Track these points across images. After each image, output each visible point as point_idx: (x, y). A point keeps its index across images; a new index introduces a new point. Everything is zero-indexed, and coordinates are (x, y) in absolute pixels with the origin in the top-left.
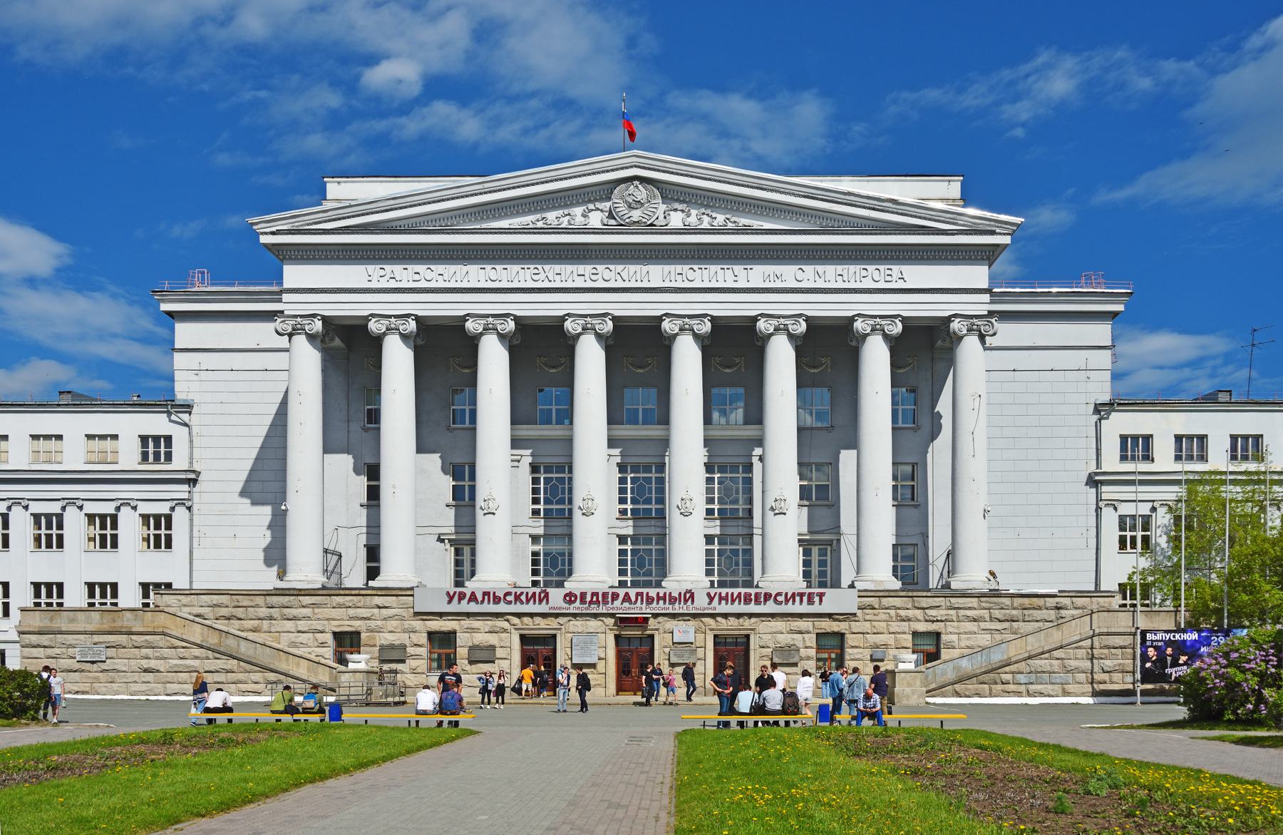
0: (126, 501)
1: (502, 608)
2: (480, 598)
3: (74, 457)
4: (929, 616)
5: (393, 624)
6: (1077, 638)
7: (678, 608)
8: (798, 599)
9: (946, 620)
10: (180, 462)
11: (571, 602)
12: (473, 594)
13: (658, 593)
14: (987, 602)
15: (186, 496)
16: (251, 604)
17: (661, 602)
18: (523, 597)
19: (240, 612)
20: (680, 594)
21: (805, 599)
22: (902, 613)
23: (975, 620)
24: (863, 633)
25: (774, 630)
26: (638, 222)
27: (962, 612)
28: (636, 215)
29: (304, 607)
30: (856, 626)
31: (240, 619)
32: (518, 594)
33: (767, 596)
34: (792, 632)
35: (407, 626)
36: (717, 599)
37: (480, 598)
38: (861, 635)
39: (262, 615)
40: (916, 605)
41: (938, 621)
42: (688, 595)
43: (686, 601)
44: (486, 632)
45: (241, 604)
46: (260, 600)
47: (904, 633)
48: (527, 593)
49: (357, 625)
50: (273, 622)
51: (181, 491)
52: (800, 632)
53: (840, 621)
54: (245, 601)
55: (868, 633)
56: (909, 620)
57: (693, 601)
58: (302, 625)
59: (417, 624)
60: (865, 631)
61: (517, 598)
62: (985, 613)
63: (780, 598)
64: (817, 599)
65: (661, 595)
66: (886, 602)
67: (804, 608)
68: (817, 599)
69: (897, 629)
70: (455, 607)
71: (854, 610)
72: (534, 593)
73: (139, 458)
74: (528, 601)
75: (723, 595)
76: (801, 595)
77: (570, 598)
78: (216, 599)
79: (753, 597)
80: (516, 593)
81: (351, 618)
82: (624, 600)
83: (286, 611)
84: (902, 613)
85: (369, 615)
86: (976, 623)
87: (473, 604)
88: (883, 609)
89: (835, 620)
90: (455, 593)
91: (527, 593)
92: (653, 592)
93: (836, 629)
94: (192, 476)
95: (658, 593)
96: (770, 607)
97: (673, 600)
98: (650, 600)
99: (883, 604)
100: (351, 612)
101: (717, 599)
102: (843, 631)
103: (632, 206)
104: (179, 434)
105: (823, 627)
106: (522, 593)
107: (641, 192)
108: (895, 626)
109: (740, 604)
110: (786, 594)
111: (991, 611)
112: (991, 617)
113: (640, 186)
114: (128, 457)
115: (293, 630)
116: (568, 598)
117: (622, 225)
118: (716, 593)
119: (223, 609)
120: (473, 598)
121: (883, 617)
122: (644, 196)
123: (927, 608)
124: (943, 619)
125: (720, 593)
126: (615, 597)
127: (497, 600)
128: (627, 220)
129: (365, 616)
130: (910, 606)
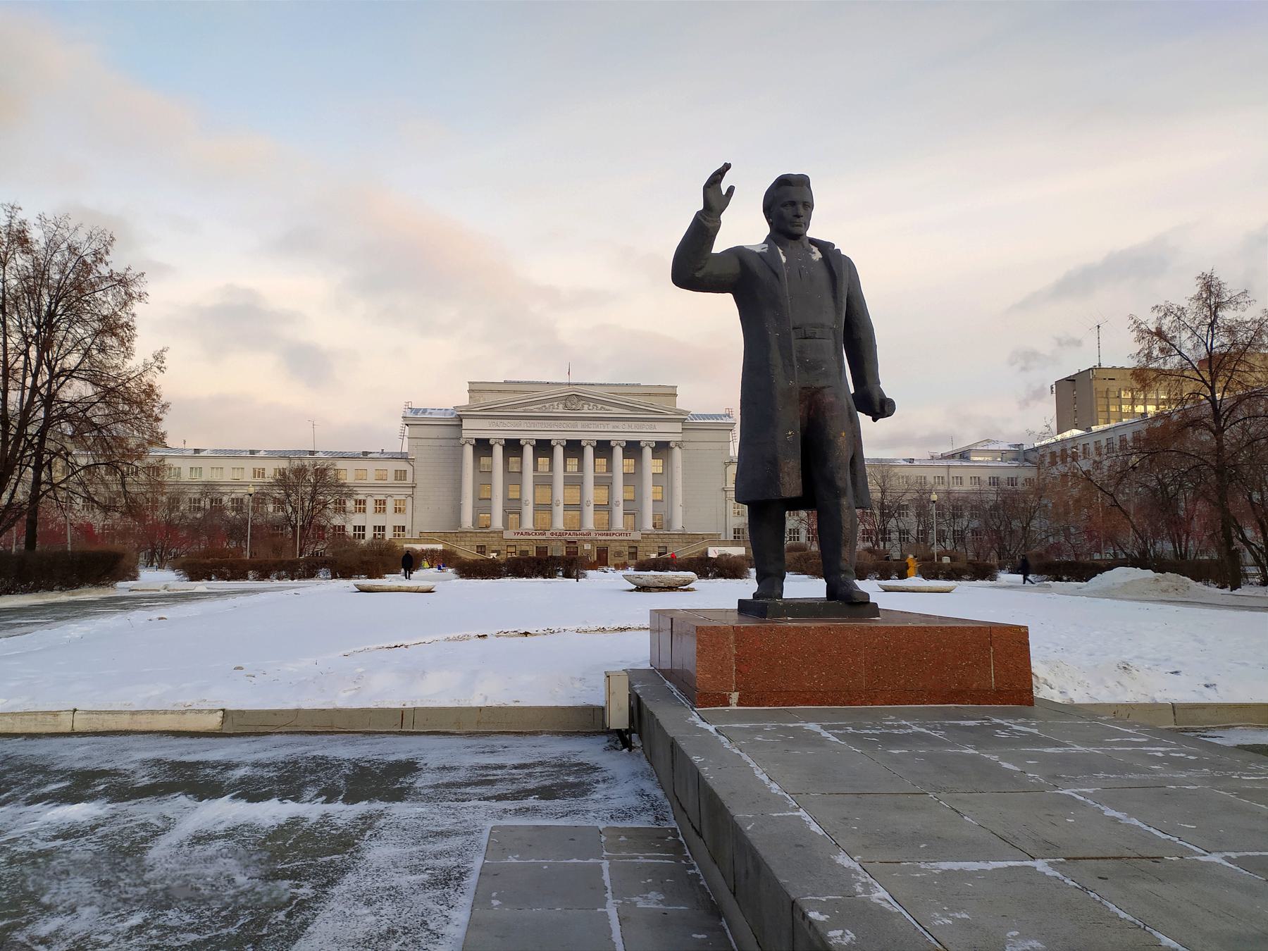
1: (531, 537)
3: (371, 479)
10: (409, 480)
33: (613, 534)
49: (485, 543)
51: (409, 491)
59: (504, 543)
61: (536, 534)
67: (625, 538)
77: (552, 534)
92: (578, 533)
96: (614, 537)
97: (584, 535)
98: (577, 535)
104: (409, 470)
114: (391, 479)
120: (522, 534)
126: (566, 534)
127: (529, 535)
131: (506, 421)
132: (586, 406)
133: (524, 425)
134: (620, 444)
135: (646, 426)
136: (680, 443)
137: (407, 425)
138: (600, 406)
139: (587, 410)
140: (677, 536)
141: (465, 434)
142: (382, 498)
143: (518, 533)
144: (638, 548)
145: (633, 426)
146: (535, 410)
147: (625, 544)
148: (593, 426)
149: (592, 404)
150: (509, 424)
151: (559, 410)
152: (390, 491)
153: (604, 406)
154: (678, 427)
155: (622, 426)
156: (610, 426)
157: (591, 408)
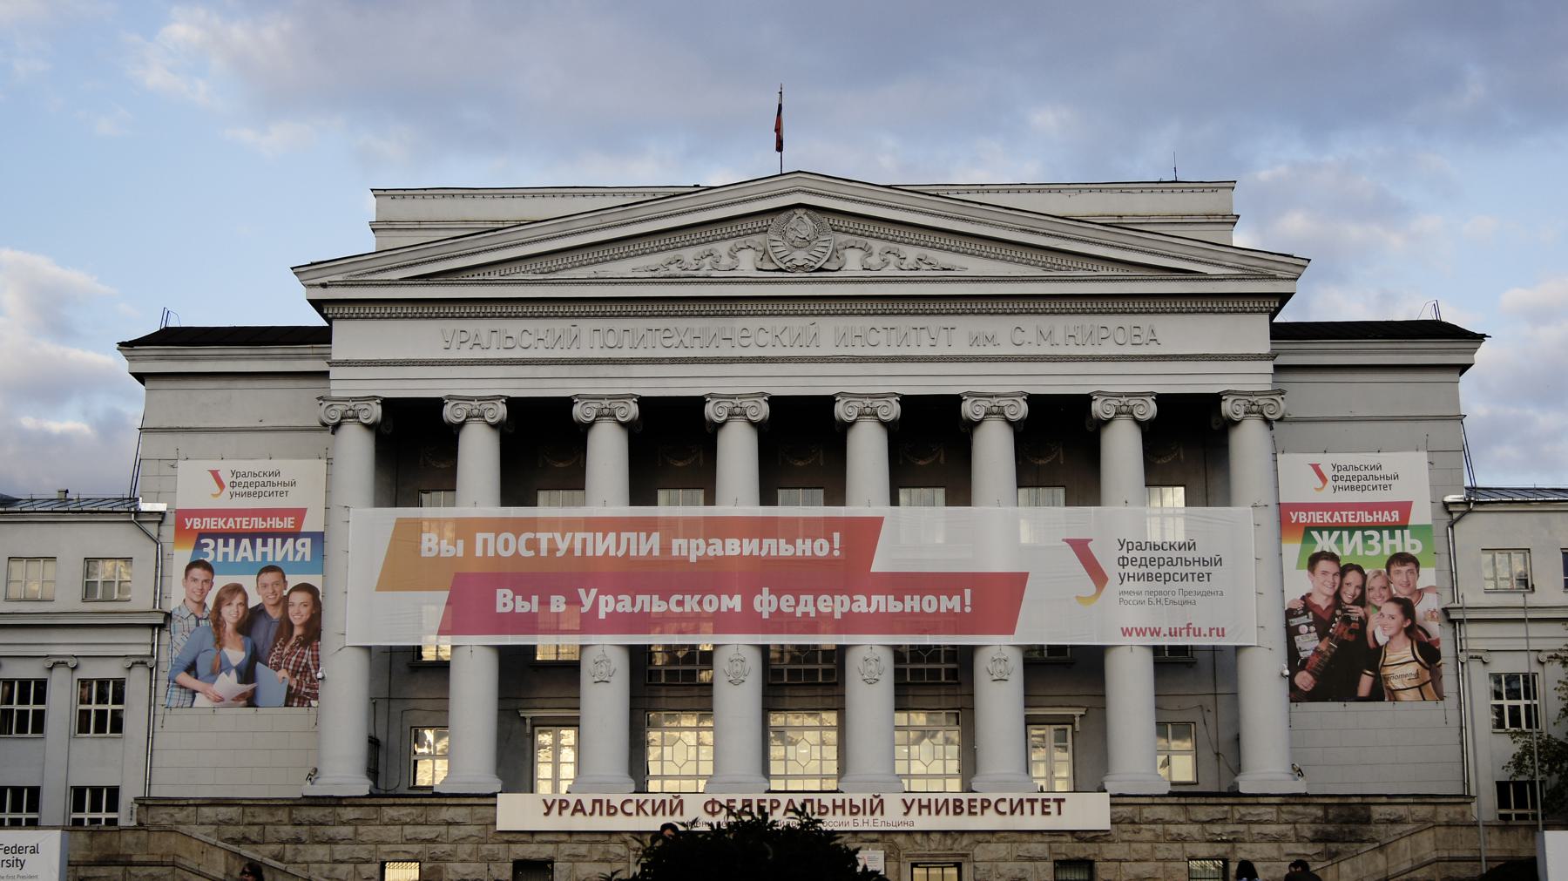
0: (61, 660)
2: (588, 809)
4: (1211, 834)
5: (465, 850)
6: (1407, 866)
7: (864, 823)
8: (1027, 806)
9: (1235, 840)
11: (713, 813)
12: (579, 802)
13: (834, 800)
14: (1291, 812)
15: (146, 651)
16: (270, 820)
17: (839, 811)
18: (648, 808)
19: (253, 833)
20: (864, 800)
21: (1038, 806)
22: (1173, 829)
23: (1276, 840)
24: (1120, 861)
25: (994, 856)
26: (803, 266)
27: (1256, 829)
28: (800, 257)
29: (343, 824)
30: (1111, 851)
31: (255, 843)
32: (641, 803)
33: (986, 805)
34: (1019, 858)
35: (486, 853)
36: (915, 807)
37: (588, 809)
38: (1118, 863)
39: (284, 837)
40: (1193, 817)
41: (1223, 841)
42: (876, 801)
43: (872, 812)
44: (595, 861)
45: (256, 821)
46: (282, 815)
47: (1177, 860)
48: (653, 801)
50: (300, 847)
51: (138, 643)
52: (1031, 859)
53: (1086, 841)
54: (263, 816)
55: (1127, 861)
56: (1184, 840)
57: (882, 813)
58: (341, 851)
59: (499, 849)
60: (1122, 858)
61: (640, 807)
62: (1284, 827)
63: (1004, 807)
64: (1053, 807)
65: (839, 803)
66: (1147, 813)
68: (1053, 807)
69: (1166, 854)
70: (557, 822)
71: (1106, 825)
72: (663, 802)
73: (78, 591)
74: (654, 813)
75: (924, 803)
76: (1032, 801)
78: (224, 813)
79: (965, 806)
80: (638, 801)
81: (409, 841)
82: (787, 810)
83: (319, 830)
84: (1173, 829)
85: (433, 836)
86: (1276, 845)
87: (579, 815)
88: (1146, 823)
89: (1081, 840)
90: (554, 801)
91: (653, 801)
93: (1082, 855)
94: (161, 621)
95: (834, 800)
96: (989, 821)
97: (855, 810)
99: (1145, 815)
100: (409, 830)
101: (915, 807)
102: (1091, 858)
103: (795, 244)
105: (1063, 851)
106: (646, 801)
107: (804, 225)
108: (1163, 850)
109: (947, 813)
110: (1011, 800)
111: (1297, 826)
112: (1297, 835)
113: (806, 217)
115: (327, 858)
116: (709, 808)
117: (780, 270)
118: (913, 800)
119: (231, 828)
121: (1147, 835)
122: (810, 230)
123: (1208, 822)
124: (1231, 838)
125: (920, 800)
127: (611, 811)
128: (788, 264)
129: (427, 837)
130: (1182, 819)
131: (513, 327)
132: (853, 262)
133: (590, 337)
134: (1001, 413)
135: (1115, 333)
136: (1262, 401)
137: (141, 377)
138: (911, 253)
140: (1268, 813)
141: (343, 384)
142: (32, 671)
143: (564, 803)
144: (1100, 866)
145: (1063, 332)
147: (1038, 848)
148: (883, 334)
149: (877, 246)
152: (62, 645)
153: (933, 255)
154: (1253, 333)
155: (1004, 333)
156: (960, 333)
157: (874, 261)
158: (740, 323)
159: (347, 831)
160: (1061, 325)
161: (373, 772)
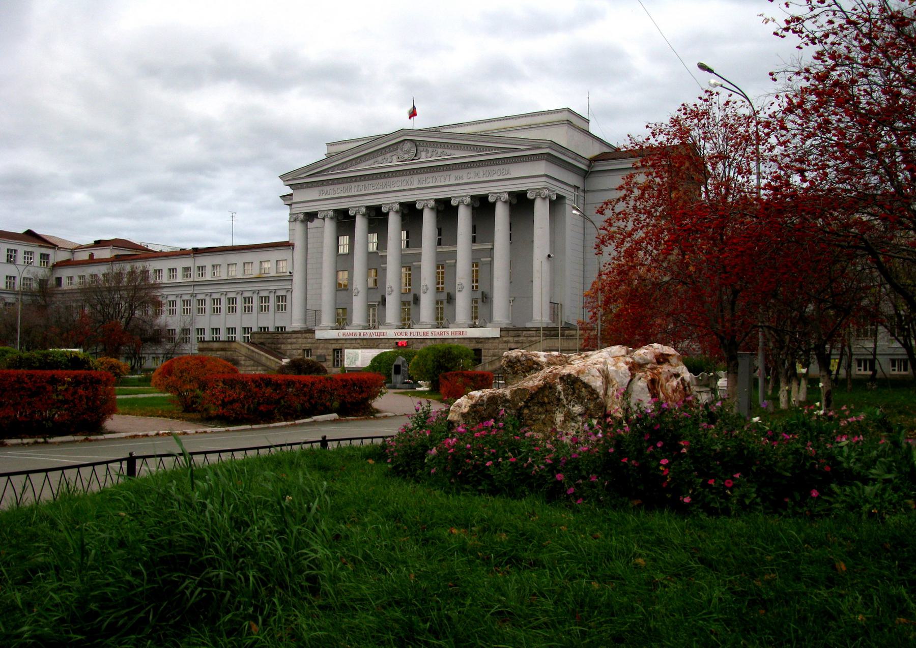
28: (406, 157)
58: (294, 346)
131: (335, 187)
132: (423, 154)
135: (497, 172)
138: (440, 151)
139: (426, 158)
145: (480, 174)
146: (364, 168)
148: (430, 180)
149: (430, 150)
150: (339, 190)
151: (392, 162)
155: (466, 176)
156: (451, 178)
158: (392, 179)
159: (294, 340)
160: (481, 170)
161: (306, 323)
